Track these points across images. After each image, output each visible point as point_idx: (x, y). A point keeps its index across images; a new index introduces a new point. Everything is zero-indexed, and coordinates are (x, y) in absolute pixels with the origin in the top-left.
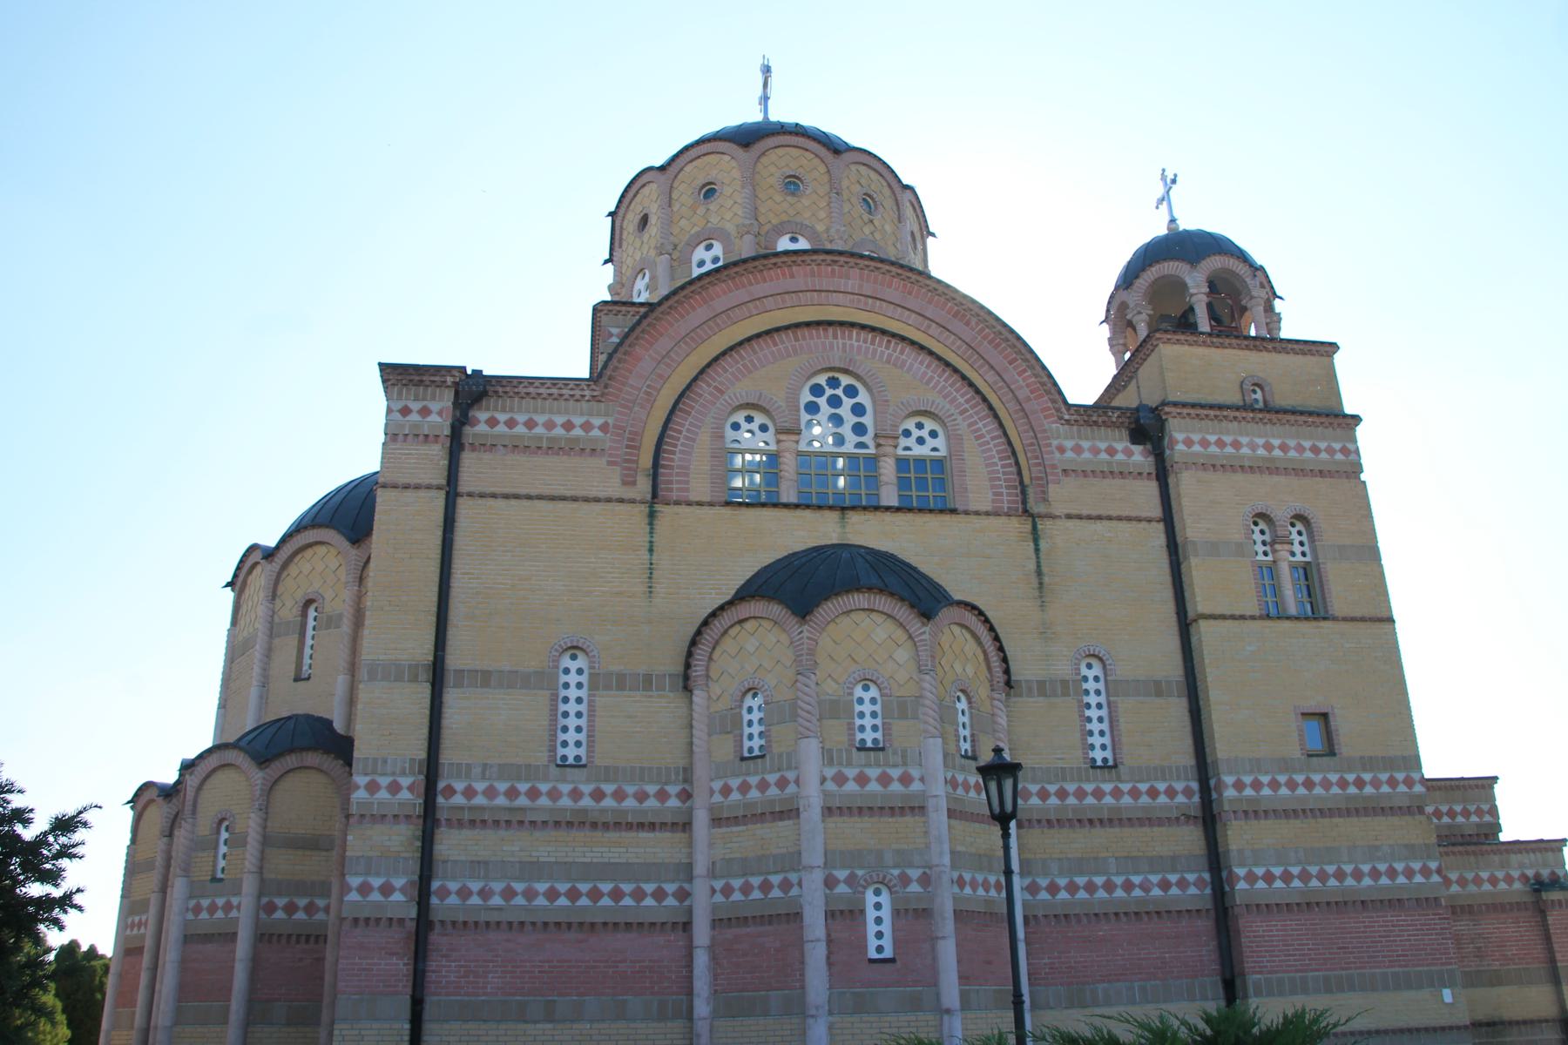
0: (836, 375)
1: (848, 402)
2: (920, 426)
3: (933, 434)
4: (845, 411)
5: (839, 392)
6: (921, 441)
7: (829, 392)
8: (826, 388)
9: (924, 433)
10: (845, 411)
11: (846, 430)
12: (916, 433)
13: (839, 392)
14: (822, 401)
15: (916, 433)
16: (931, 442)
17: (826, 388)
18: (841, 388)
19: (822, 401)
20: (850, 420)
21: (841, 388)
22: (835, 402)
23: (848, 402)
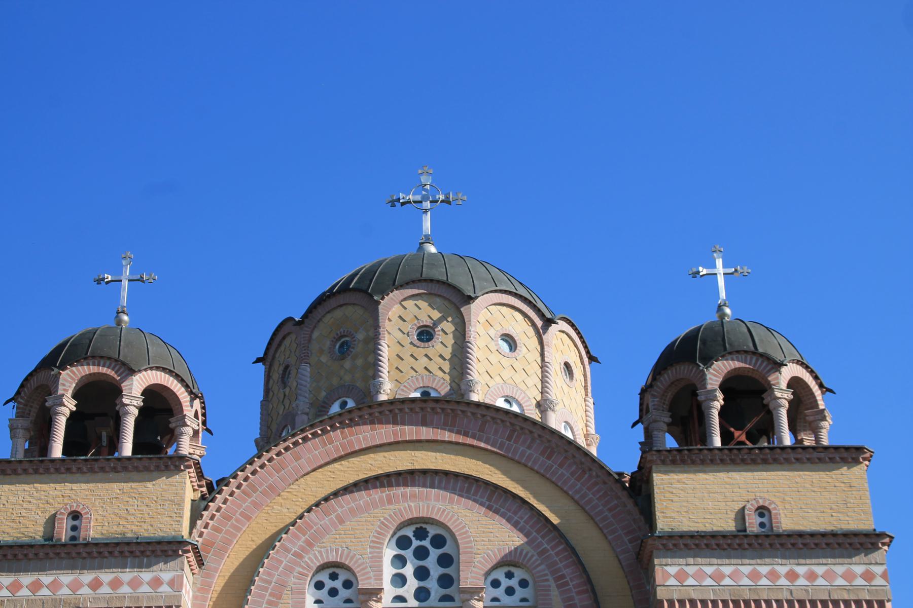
0: (424, 526)
1: (434, 553)
2: (509, 575)
3: (523, 584)
4: (431, 562)
5: (426, 543)
6: (510, 591)
7: (416, 543)
8: (413, 539)
9: (514, 583)
10: (431, 562)
11: (432, 584)
12: (505, 583)
13: (426, 543)
14: (408, 554)
15: (505, 583)
16: (520, 592)
17: (413, 539)
18: (428, 539)
19: (408, 554)
20: (436, 571)
21: (428, 539)
22: (421, 553)
23: (434, 553)
